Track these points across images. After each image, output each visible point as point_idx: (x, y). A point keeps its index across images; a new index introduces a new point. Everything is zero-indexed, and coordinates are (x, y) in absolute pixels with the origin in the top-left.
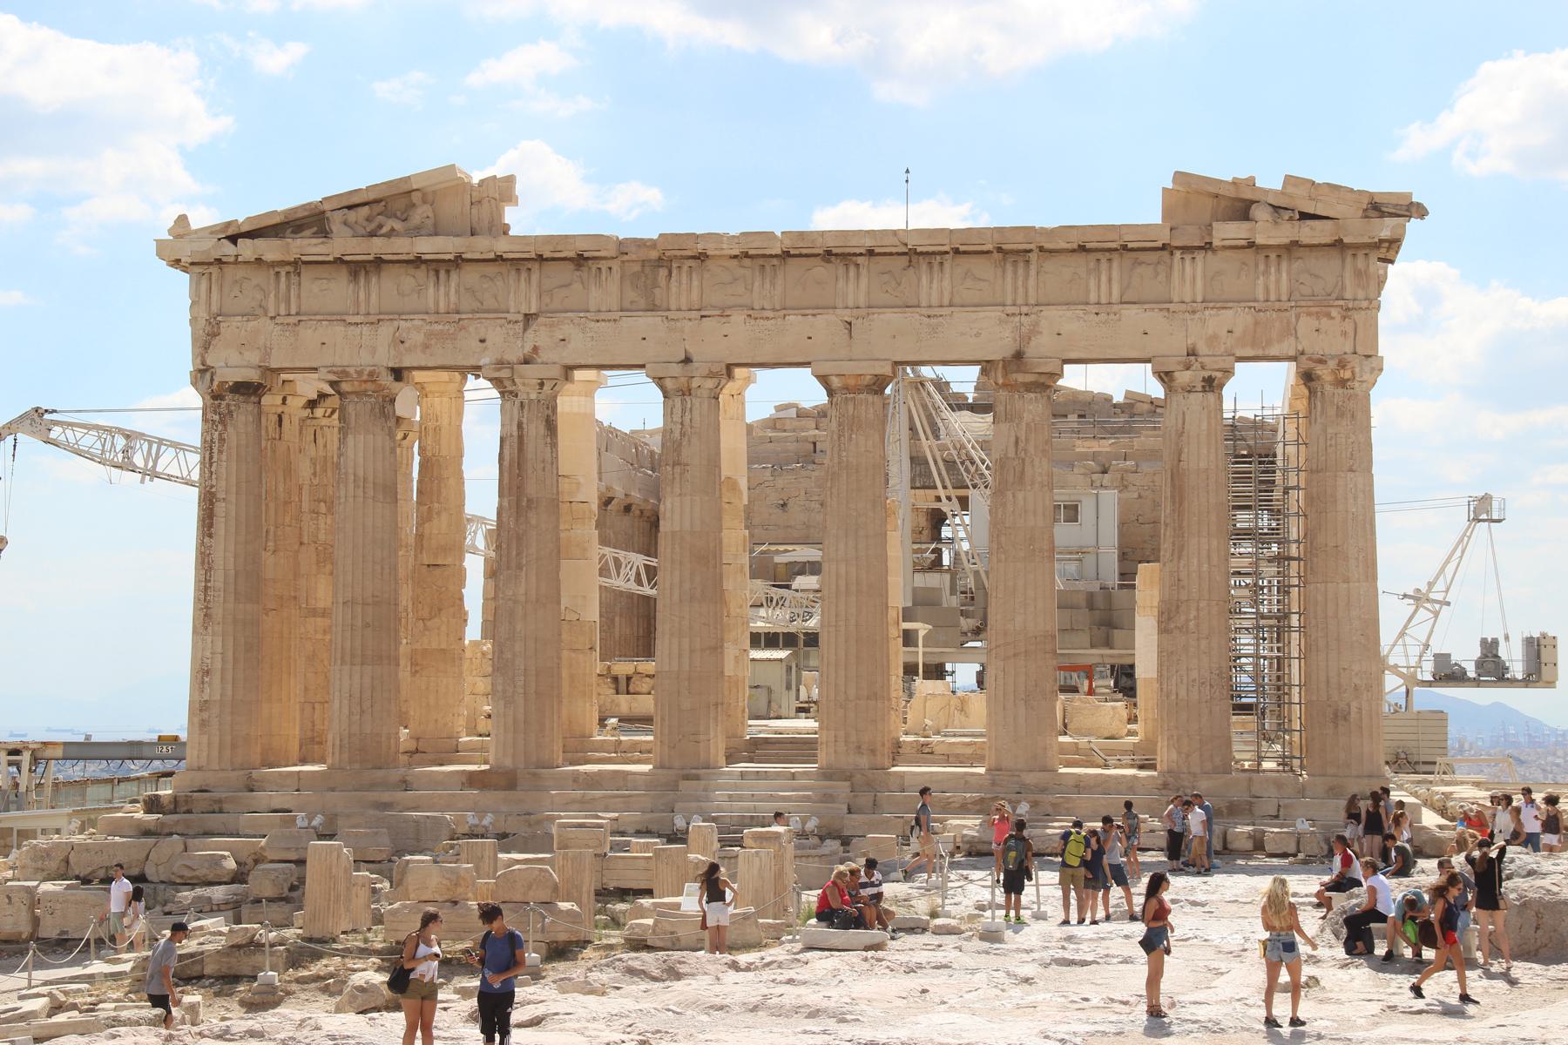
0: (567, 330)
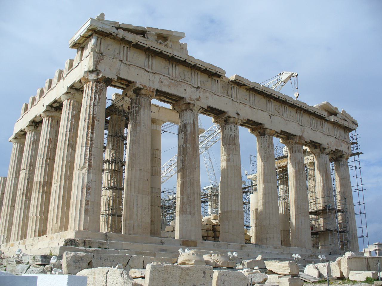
0: (208, 94)
